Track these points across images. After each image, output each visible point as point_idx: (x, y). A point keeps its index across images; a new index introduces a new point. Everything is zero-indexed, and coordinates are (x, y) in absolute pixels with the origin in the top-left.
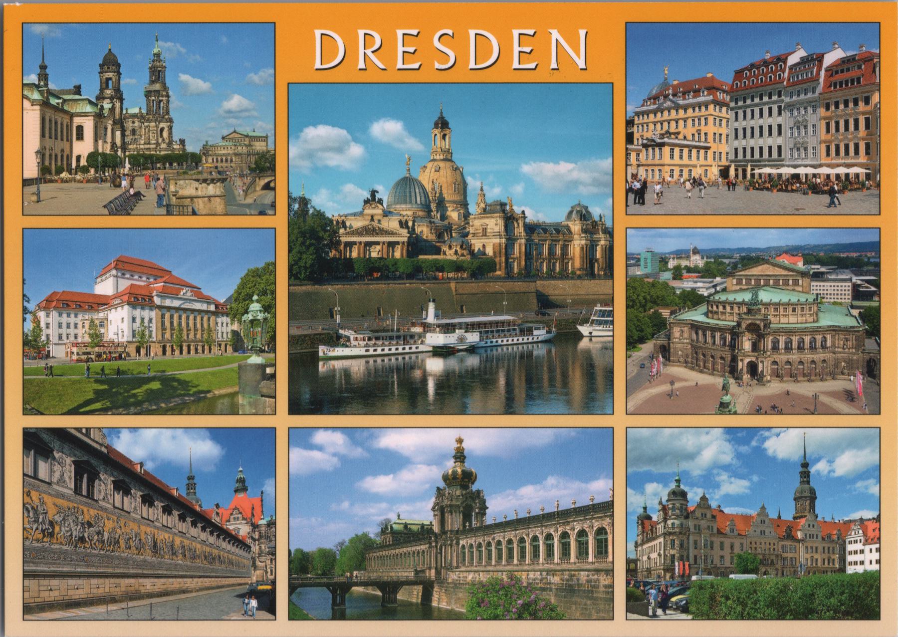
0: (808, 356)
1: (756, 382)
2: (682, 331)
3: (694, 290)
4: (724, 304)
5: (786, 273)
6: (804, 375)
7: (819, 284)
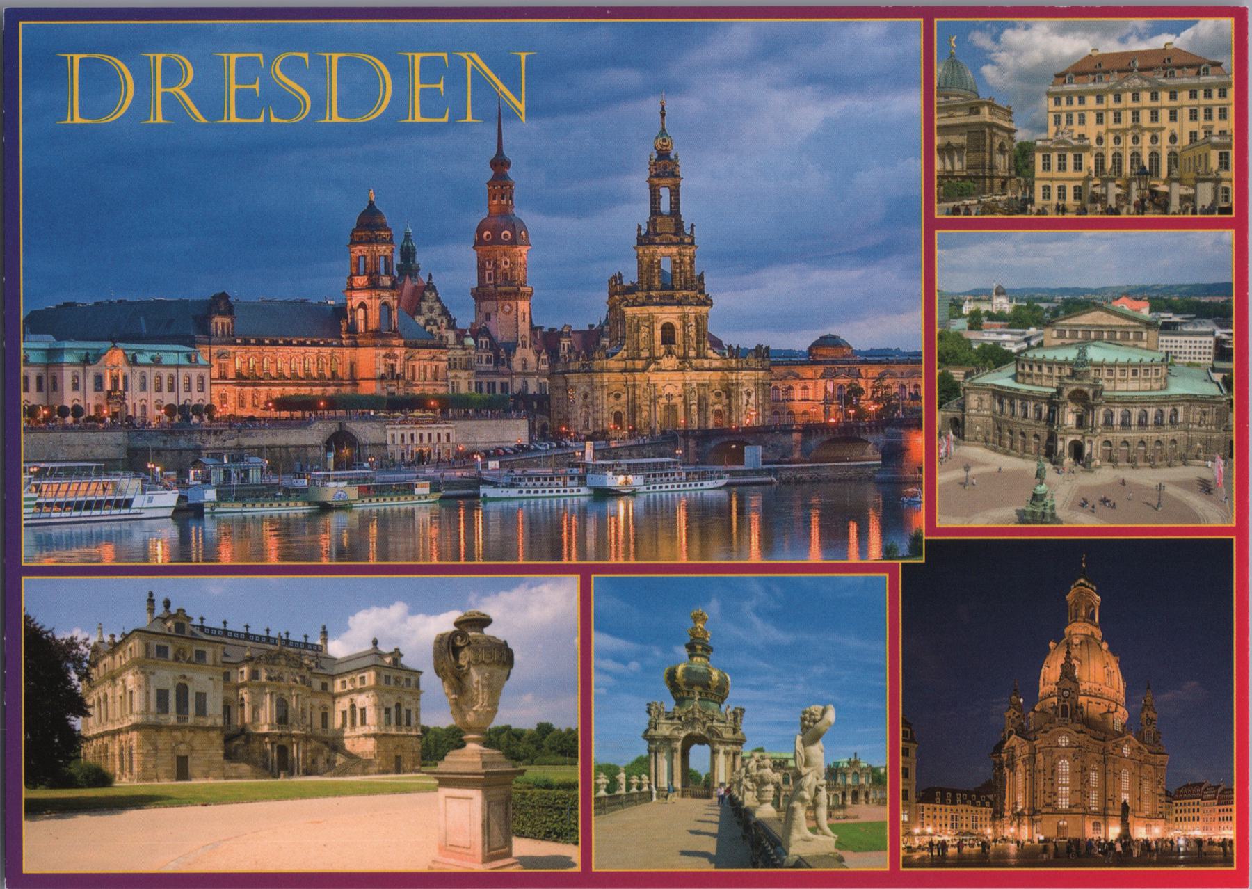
0: (1151, 435)
1: (1080, 467)
2: (981, 400)
3: (997, 344)
4: (1040, 363)
5: (1126, 322)
6: (1146, 460)
7: (1169, 338)
